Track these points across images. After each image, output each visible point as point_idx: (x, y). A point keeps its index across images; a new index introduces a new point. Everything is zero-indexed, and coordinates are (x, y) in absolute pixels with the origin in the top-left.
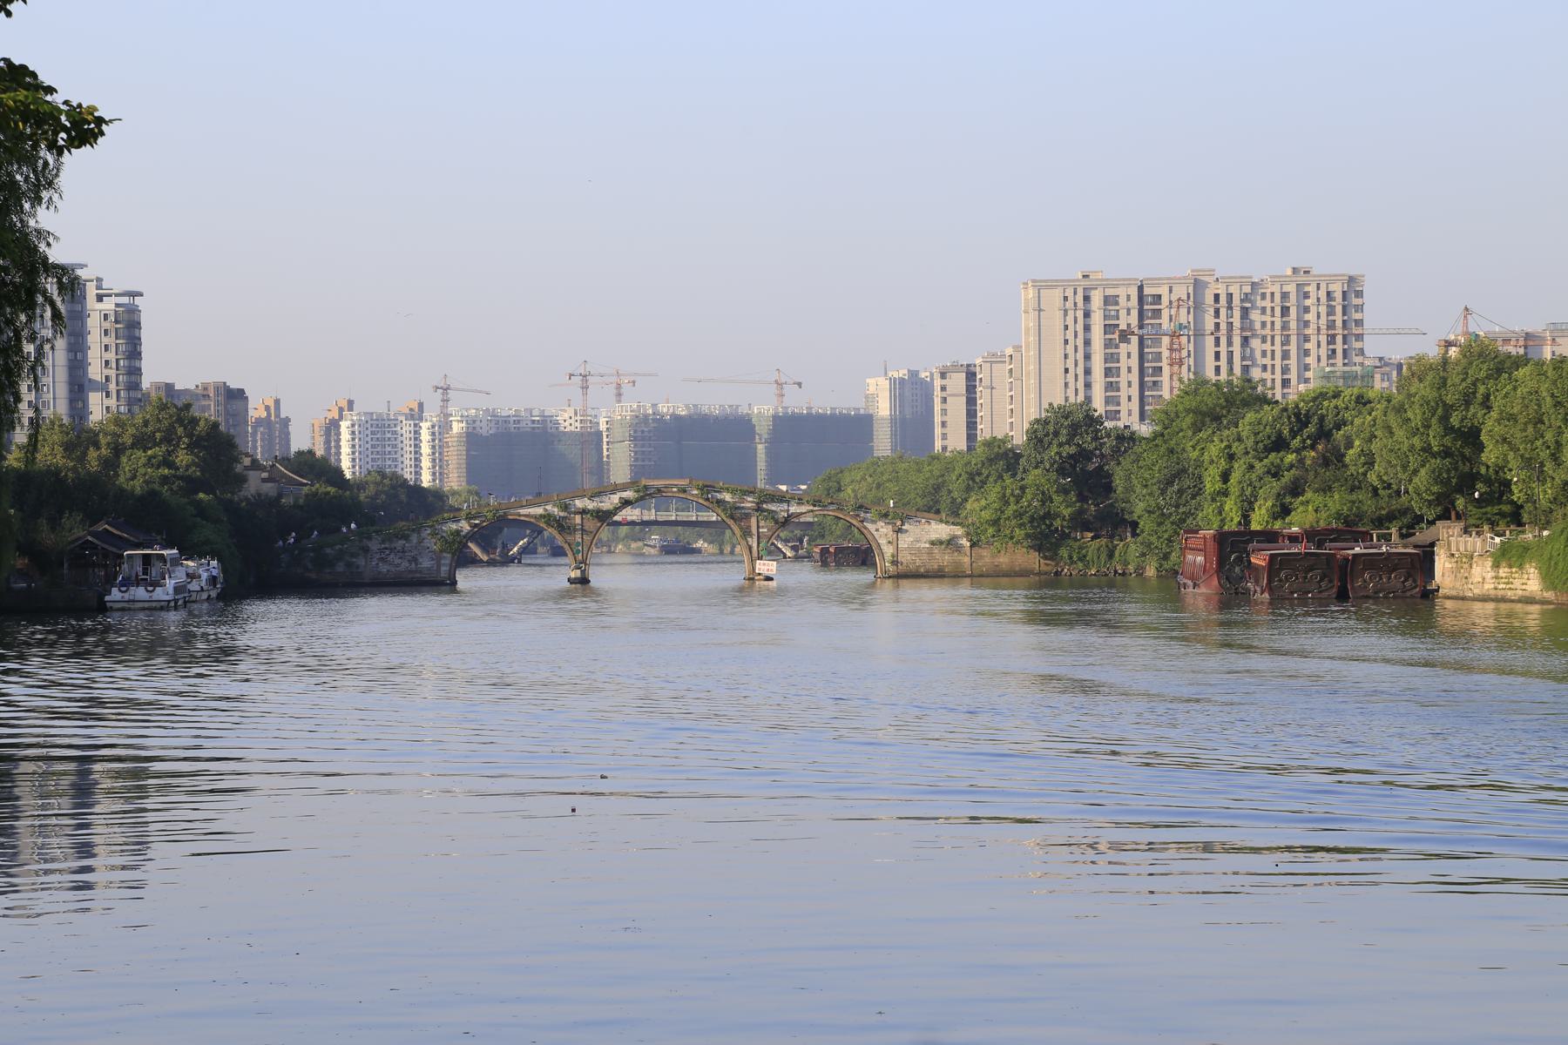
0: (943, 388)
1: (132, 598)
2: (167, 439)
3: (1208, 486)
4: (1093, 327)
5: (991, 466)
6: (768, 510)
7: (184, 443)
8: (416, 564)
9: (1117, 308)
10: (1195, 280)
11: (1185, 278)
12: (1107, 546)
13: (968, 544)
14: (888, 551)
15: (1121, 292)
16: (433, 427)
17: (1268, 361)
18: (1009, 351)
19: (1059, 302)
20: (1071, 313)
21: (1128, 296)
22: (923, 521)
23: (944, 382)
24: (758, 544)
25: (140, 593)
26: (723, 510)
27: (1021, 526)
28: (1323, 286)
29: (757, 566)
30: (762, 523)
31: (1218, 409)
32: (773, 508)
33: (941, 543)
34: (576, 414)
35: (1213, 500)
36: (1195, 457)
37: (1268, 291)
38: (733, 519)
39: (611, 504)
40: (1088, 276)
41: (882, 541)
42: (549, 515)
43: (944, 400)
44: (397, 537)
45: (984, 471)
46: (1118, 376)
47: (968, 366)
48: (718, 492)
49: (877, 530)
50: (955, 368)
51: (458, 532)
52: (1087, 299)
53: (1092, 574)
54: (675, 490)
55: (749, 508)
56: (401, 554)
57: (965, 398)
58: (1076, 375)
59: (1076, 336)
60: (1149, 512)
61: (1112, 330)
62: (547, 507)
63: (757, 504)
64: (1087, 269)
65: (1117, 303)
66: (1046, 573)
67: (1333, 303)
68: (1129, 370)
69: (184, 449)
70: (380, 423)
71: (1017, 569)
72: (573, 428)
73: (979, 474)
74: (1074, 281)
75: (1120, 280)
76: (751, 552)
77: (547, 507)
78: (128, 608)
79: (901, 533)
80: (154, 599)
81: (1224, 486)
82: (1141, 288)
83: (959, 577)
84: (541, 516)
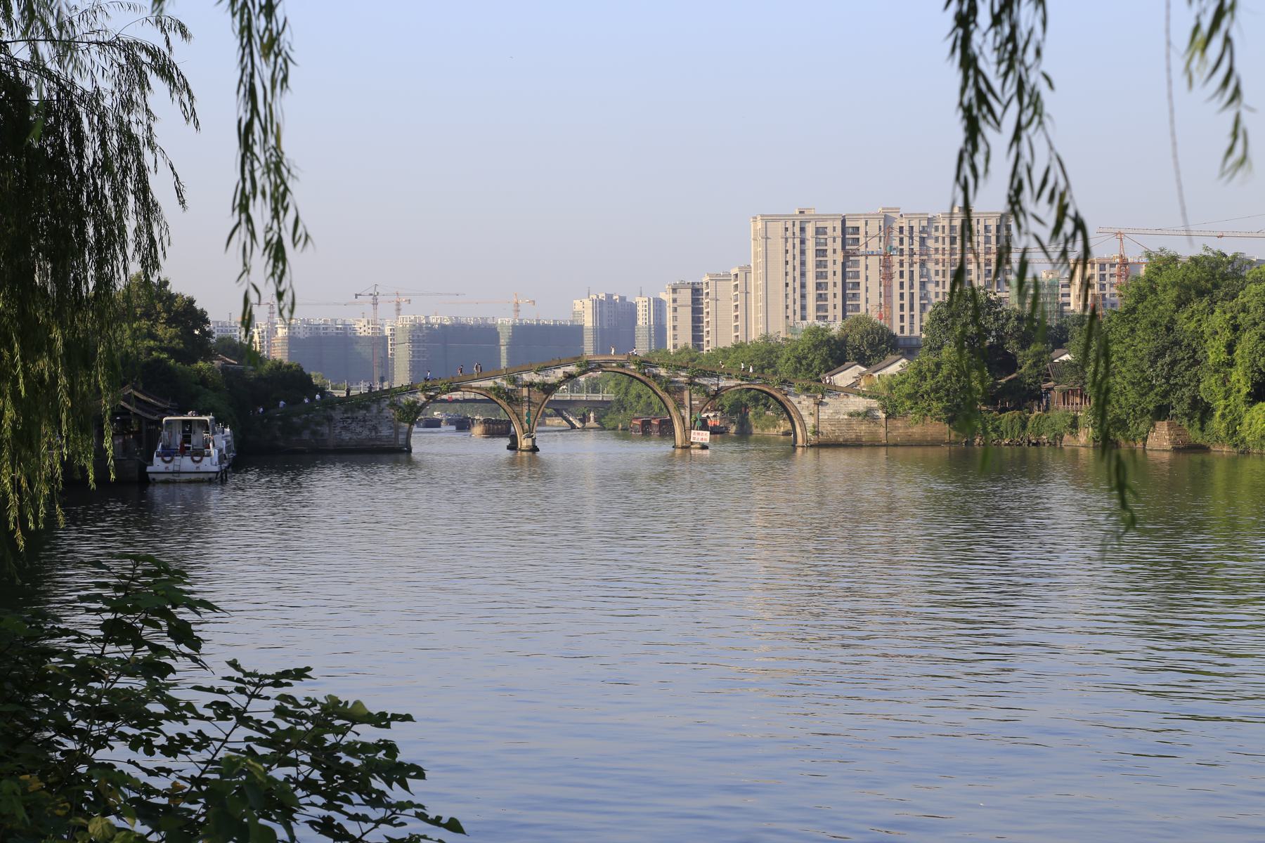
0: (675, 301)
1: (177, 469)
2: (147, 315)
3: (1212, 357)
4: (807, 252)
5: (816, 350)
6: (699, 384)
7: (163, 318)
8: (376, 433)
9: (826, 237)
10: (885, 216)
11: (878, 214)
12: (1020, 418)
13: (884, 416)
14: (810, 421)
15: (829, 225)
16: (263, 332)
17: (940, 278)
18: (735, 271)
19: (781, 231)
20: (790, 241)
21: (834, 228)
22: (842, 394)
23: (675, 296)
24: (691, 417)
25: (186, 463)
26: (659, 384)
27: (939, 399)
28: (982, 221)
29: (692, 436)
30: (694, 396)
31: (1203, 282)
32: (705, 383)
33: (859, 414)
34: (368, 323)
35: (1217, 371)
36: (1192, 328)
37: (940, 225)
40: (803, 212)
41: (804, 413)
42: (499, 387)
43: (675, 310)
44: (359, 408)
45: (811, 357)
46: (826, 289)
47: (693, 284)
48: (654, 367)
49: (800, 403)
50: (683, 285)
51: (415, 403)
52: (802, 230)
53: (1006, 445)
54: (614, 365)
55: (682, 382)
56: (362, 423)
57: (690, 308)
58: (794, 289)
59: (794, 259)
60: (1133, 384)
61: (821, 254)
62: (497, 380)
63: (690, 378)
64: (803, 207)
65: (825, 233)
66: (957, 443)
67: (990, 234)
68: (835, 285)
69: (164, 323)
70: (224, 329)
71: (929, 439)
72: (366, 334)
73: (805, 358)
74: (793, 216)
75: (827, 215)
76: (684, 423)
77: (497, 380)
78: (171, 481)
79: (822, 405)
80: (201, 470)
81: (1229, 357)
82: (844, 222)
83: (875, 446)
84: (491, 388)
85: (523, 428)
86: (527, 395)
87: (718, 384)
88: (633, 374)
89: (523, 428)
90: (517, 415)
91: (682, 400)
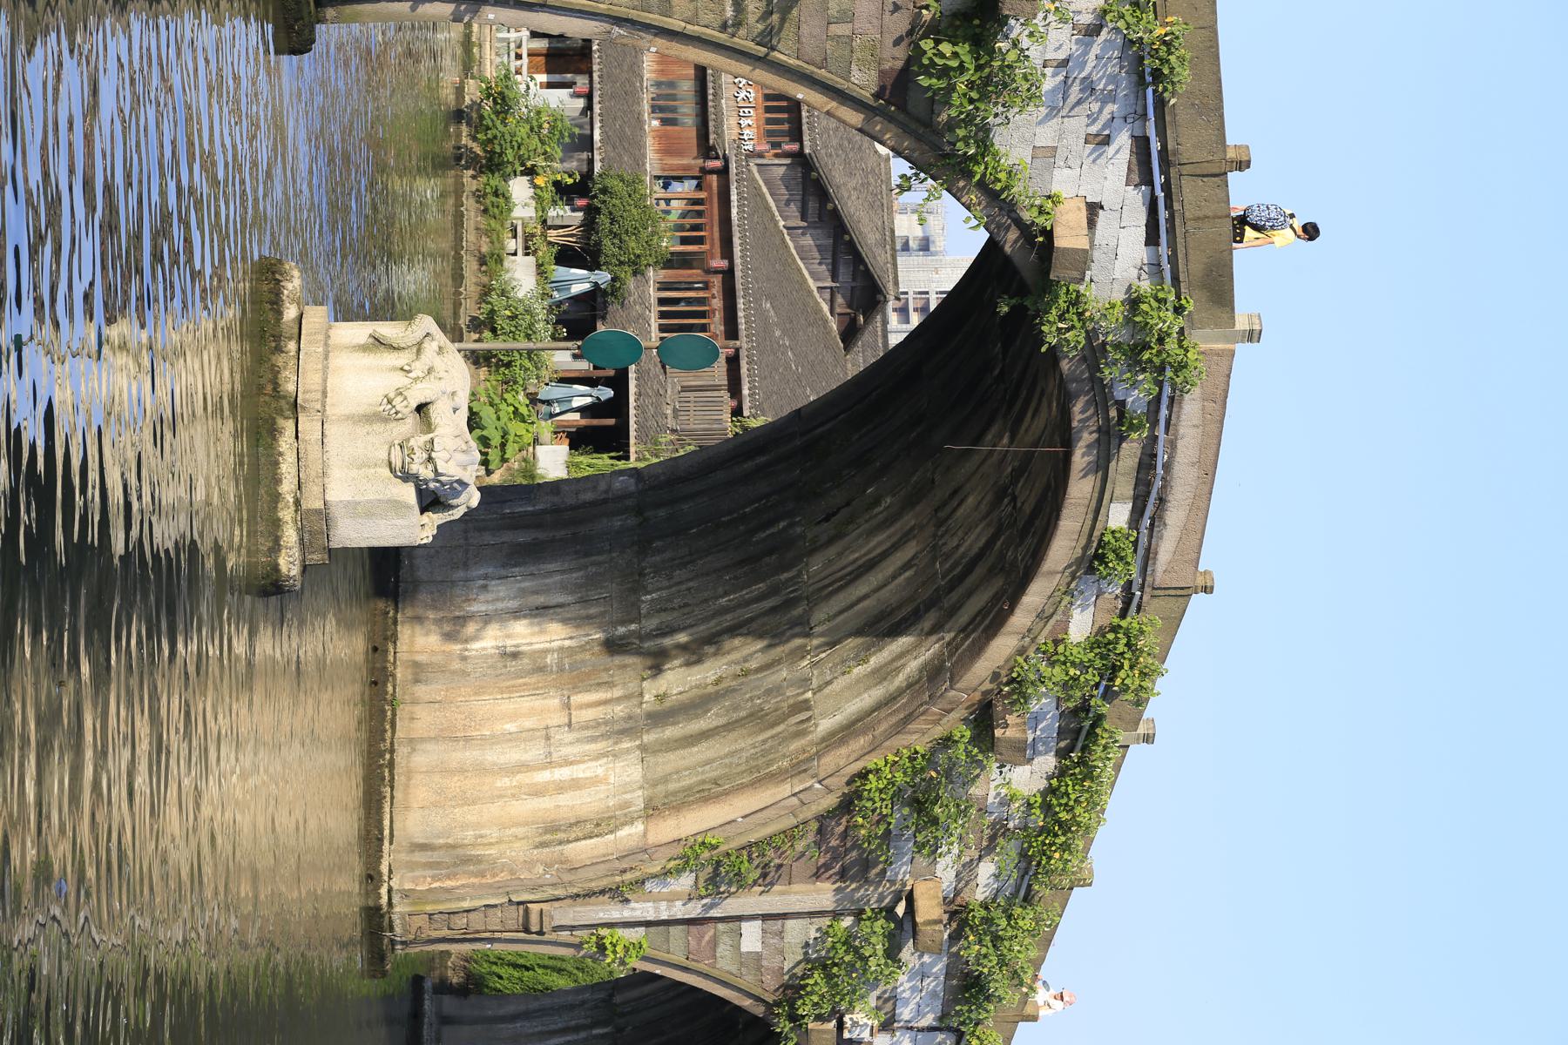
38: (847, 805)
39: (1047, 155)
54: (1118, 516)
87: (887, 1026)
88: (1021, 618)
91: (767, 877)
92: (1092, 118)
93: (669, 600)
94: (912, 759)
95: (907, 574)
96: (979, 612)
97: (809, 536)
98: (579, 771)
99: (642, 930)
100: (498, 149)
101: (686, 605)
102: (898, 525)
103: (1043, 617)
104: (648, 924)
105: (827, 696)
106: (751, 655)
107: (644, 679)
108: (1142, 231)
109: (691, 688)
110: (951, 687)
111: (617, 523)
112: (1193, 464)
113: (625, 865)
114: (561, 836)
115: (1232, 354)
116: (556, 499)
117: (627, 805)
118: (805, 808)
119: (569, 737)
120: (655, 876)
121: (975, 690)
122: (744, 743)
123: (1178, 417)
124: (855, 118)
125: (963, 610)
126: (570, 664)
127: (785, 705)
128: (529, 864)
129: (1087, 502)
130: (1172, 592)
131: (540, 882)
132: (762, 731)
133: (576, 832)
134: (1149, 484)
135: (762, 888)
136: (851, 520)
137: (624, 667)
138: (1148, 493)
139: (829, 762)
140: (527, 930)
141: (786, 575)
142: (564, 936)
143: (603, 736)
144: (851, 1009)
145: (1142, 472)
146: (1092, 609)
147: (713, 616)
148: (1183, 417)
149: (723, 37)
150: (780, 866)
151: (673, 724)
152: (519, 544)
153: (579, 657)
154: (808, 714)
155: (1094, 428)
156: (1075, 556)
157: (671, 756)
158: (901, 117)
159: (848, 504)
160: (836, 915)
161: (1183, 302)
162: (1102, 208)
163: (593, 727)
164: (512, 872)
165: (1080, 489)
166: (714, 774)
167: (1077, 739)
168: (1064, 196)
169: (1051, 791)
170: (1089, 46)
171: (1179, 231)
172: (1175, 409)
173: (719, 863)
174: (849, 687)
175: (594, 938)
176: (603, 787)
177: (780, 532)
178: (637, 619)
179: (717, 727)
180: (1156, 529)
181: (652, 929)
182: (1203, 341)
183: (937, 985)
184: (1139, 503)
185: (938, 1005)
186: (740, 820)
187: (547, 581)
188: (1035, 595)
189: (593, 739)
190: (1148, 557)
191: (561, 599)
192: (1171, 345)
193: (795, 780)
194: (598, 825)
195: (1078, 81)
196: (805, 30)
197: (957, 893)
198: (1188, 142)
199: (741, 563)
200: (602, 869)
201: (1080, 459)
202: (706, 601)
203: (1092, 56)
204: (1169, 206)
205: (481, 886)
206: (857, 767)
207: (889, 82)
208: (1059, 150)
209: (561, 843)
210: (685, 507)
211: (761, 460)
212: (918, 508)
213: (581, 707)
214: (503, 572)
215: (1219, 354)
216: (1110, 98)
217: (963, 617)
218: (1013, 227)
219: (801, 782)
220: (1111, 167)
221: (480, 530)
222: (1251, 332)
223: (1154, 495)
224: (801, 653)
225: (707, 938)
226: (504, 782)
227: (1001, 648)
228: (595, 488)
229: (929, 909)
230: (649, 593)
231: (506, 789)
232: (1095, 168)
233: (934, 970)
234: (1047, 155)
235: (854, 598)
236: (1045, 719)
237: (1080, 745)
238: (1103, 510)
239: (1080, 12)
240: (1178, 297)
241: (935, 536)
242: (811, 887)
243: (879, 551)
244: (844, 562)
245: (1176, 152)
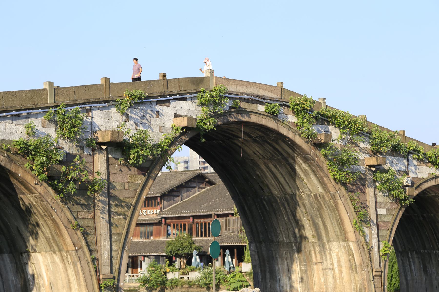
38: (344, 184)
39: (161, 128)
54: (261, 108)
85: (97, 270)
86: (104, 176)
87: (407, 173)
88: (290, 135)
89: (97, 270)
90: (85, 234)
91: (365, 207)
92: (151, 116)
93: (285, 234)
94: (330, 166)
95: (278, 167)
96: (289, 147)
97: (267, 194)
98: (335, 260)
99: (380, 242)
100: (159, 282)
101: (287, 229)
102: (264, 169)
103: (290, 129)
104: (379, 241)
105: (313, 189)
106: (301, 211)
107: (308, 242)
108: (183, 102)
109: (311, 228)
110: (310, 154)
111: (264, 249)
112: (247, 88)
113: (362, 247)
114: (354, 266)
115: (216, 77)
116: (257, 266)
117: (344, 246)
118: (345, 196)
119: (325, 263)
120: (365, 239)
121: (311, 148)
122: (326, 213)
123: (234, 92)
124: (151, 182)
125: (288, 151)
126: (304, 262)
127: (315, 201)
128: (362, 275)
129: (258, 117)
130: (283, 93)
131: (367, 272)
132: (323, 208)
133: (352, 261)
134: (253, 100)
135: (368, 208)
136: (263, 183)
137: (305, 247)
138: (255, 100)
139: (331, 189)
140: (381, 276)
141: (279, 201)
142: (382, 265)
143: (325, 253)
144: (403, 183)
145: (249, 102)
146: (288, 116)
147: (290, 222)
148: (234, 91)
149: (128, 219)
150: (362, 203)
151: (321, 233)
152: (270, 277)
153: (302, 260)
154: (318, 195)
155: (237, 115)
156: (273, 120)
157: (330, 234)
158: (150, 169)
159: (258, 184)
160: (375, 187)
161: (202, 91)
162: (176, 113)
163: (322, 256)
164: (364, 280)
165: (254, 119)
166: (335, 222)
167: (324, 120)
168: (173, 124)
169: (339, 127)
170: (131, 117)
171: (182, 92)
172: (232, 93)
173: (361, 221)
174: (310, 183)
175: (383, 256)
176: (339, 253)
177: (266, 203)
178: (291, 243)
179: (322, 221)
180: (265, 98)
181: (380, 240)
182: (213, 85)
183: (395, 159)
184: (258, 102)
185: (401, 159)
186: (348, 214)
187: (281, 269)
188: (284, 131)
189: (326, 256)
190: (273, 100)
191: (286, 265)
192: (214, 94)
193: (337, 198)
194: (350, 255)
195: (141, 120)
196: (126, 196)
197: (368, 153)
198: (158, 90)
199: (275, 213)
200: (363, 254)
201: (245, 119)
202: (286, 224)
203: (134, 116)
204: (176, 95)
205: (368, 289)
206: (333, 181)
207: (141, 172)
208: (160, 125)
209: (356, 266)
210: (259, 229)
211: (246, 208)
212: (260, 164)
213: (316, 260)
214: (278, 281)
215: (216, 81)
216: (146, 111)
217: (290, 151)
218: (181, 138)
219: (337, 197)
220: (165, 111)
221: (266, 288)
222: (211, 72)
223: (256, 99)
224: (301, 197)
225: (382, 224)
226: (338, 281)
227: (299, 141)
228: (254, 255)
229: (373, 161)
230: (284, 240)
231: (340, 281)
232: (165, 115)
233: (391, 160)
234: (161, 128)
235: (285, 182)
236: (319, 128)
237: (326, 119)
238: (260, 112)
239: (122, 120)
240: (201, 92)
241: (267, 159)
242: (367, 195)
243: (271, 175)
244: (275, 185)
245: (161, 93)
